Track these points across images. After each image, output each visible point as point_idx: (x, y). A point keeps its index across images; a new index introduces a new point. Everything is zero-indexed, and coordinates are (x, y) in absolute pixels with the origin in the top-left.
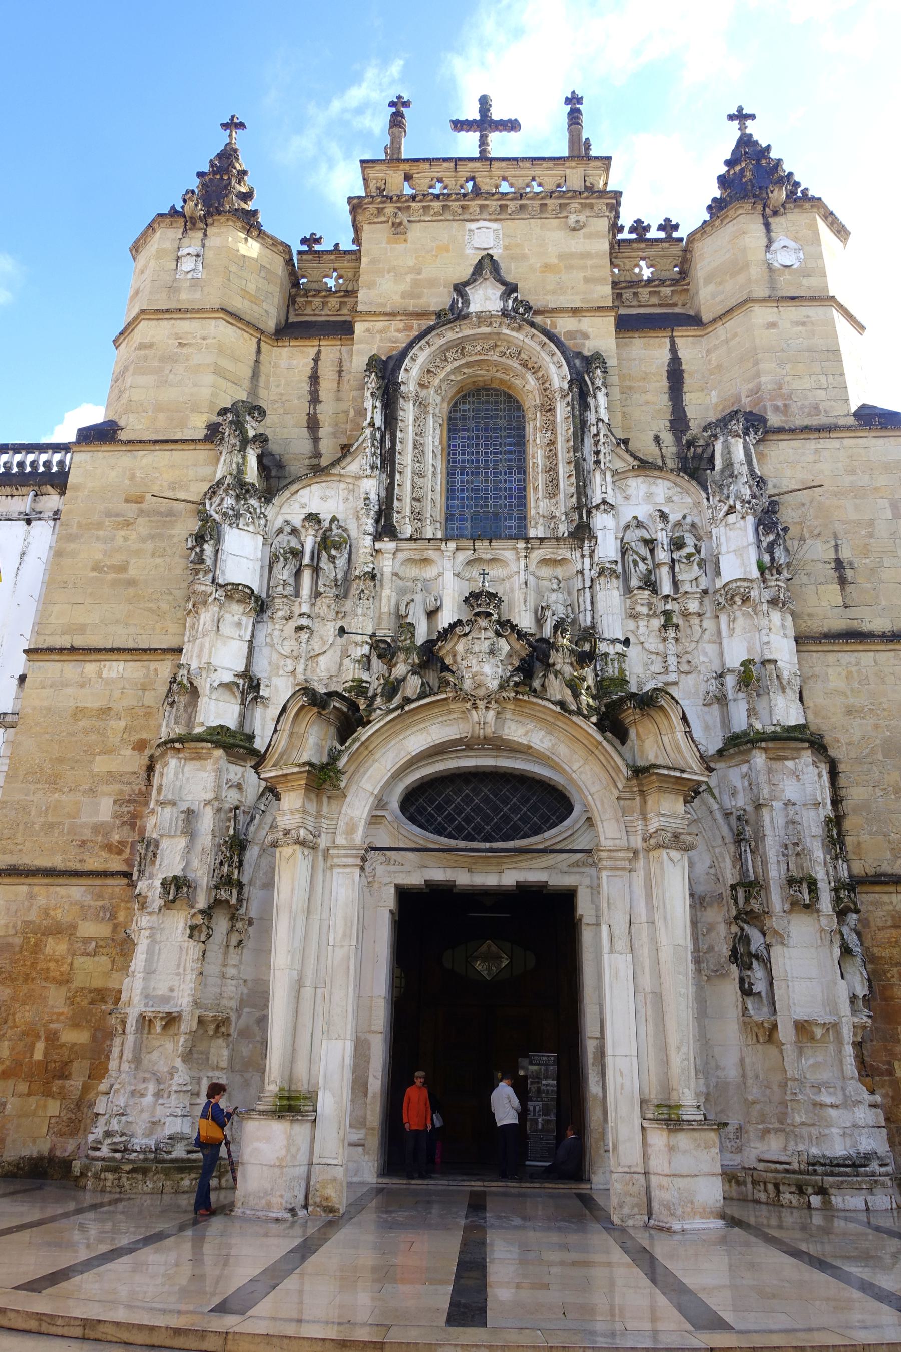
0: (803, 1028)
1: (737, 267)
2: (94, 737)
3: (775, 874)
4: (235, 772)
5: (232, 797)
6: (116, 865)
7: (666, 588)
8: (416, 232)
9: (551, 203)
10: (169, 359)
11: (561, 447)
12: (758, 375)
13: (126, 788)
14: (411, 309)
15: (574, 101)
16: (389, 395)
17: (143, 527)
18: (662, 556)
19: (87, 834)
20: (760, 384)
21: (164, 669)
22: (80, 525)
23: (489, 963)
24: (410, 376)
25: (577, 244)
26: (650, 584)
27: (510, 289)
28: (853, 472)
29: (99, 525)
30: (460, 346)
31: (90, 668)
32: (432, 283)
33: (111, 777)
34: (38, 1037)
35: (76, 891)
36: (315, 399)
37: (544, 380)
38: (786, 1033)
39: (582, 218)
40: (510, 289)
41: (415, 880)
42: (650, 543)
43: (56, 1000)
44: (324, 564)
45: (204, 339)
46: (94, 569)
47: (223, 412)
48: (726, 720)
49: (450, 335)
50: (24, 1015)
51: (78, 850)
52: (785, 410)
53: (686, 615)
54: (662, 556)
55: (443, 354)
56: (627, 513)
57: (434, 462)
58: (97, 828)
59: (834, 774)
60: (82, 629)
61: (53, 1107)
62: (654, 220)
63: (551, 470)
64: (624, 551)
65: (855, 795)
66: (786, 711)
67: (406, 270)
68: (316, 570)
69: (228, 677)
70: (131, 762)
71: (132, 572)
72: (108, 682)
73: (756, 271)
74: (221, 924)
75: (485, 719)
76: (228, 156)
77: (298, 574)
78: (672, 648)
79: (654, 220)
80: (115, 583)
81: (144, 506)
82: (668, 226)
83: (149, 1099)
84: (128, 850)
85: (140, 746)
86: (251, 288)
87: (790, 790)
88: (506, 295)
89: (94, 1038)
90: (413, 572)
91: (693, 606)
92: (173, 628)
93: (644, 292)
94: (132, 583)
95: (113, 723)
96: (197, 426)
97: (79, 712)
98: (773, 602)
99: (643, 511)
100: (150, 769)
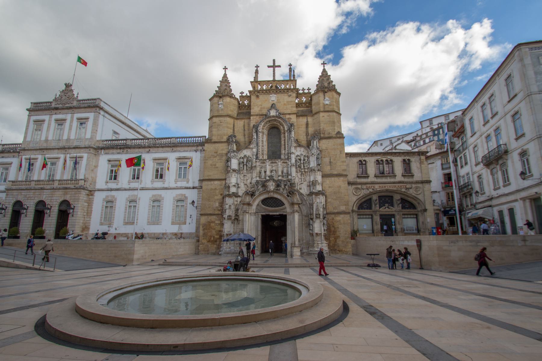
0: (317, 234)
1: (318, 104)
3: (314, 213)
4: (236, 199)
5: (236, 203)
6: (220, 213)
7: (302, 167)
8: (261, 97)
9: (285, 91)
10: (219, 125)
11: (286, 141)
15: (290, 65)
16: (257, 132)
17: (218, 158)
18: (302, 162)
21: (224, 182)
23: (276, 223)
24: (260, 129)
25: (290, 99)
26: (300, 167)
27: (277, 110)
28: (334, 145)
29: (211, 157)
30: (269, 121)
31: (212, 182)
32: (264, 108)
33: (218, 199)
35: (214, 217)
36: (244, 130)
37: (284, 127)
38: (314, 235)
40: (277, 110)
41: (264, 214)
42: (300, 160)
43: (214, 232)
46: (211, 165)
47: (229, 136)
48: (310, 189)
49: (267, 120)
50: (209, 234)
52: (324, 134)
53: (305, 172)
54: (302, 162)
55: (266, 123)
56: (297, 153)
57: (265, 143)
58: (216, 207)
59: (326, 197)
60: (210, 176)
61: (215, 246)
62: (306, 88)
63: (285, 145)
64: (296, 161)
65: (329, 200)
66: (319, 188)
67: (259, 106)
69: (234, 184)
70: (220, 197)
71: (217, 166)
73: (321, 105)
74: (236, 222)
75: (272, 195)
76: (225, 76)
77: (244, 166)
78: (303, 177)
79: (306, 88)
80: (214, 168)
82: (309, 89)
85: (221, 195)
86: (232, 109)
87: (318, 201)
88: (276, 112)
90: (262, 164)
91: (306, 170)
92: (225, 175)
93: (303, 105)
94: (217, 168)
96: (225, 139)
97: (212, 189)
98: (318, 170)
99: (299, 153)
100: (223, 198)
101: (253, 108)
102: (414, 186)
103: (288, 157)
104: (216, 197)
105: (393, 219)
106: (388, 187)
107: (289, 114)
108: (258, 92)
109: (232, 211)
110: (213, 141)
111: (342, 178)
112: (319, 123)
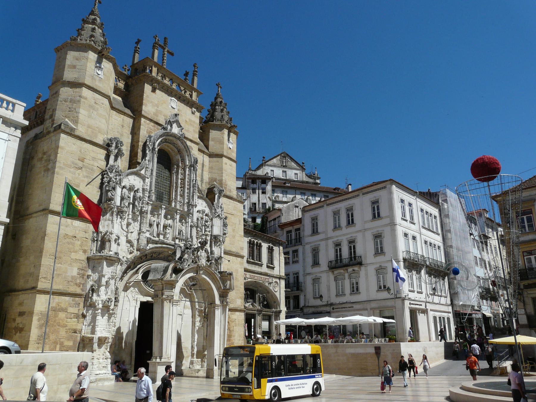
1: (222, 142)
2: (71, 246)
8: (158, 91)
10: (91, 106)
12: (222, 176)
13: (81, 265)
14: (155, 120)
19: (70, 279)
20: (222, 180)
22: (64, 164)
34: (57, 343)
35: (67, 298)
39: (195, 110)
42: (202, 218)
43: (62, 332)
44: (136, 203)
45: (102, 104)
51: (67, 284)
58: (73, 277)
63: (183, 187)
64: (198, 219)
68: (134, 205)
72: (75, 227)
81: (84, 164)
83: (101, 360)
84: (81, 286)
85: (85, 251)
89: (74, 344)
95: (76, 242)
101: (146, 105)
102: (274, 280)
103: (189, 210)
104: (73, 256)
105: (253, 320)
106: (257, 278)
107: (191, 141)
108: (157, 81)
109: (112, 291)
110: (77, 133)
111: (239, 259)
112: (221, 169)
